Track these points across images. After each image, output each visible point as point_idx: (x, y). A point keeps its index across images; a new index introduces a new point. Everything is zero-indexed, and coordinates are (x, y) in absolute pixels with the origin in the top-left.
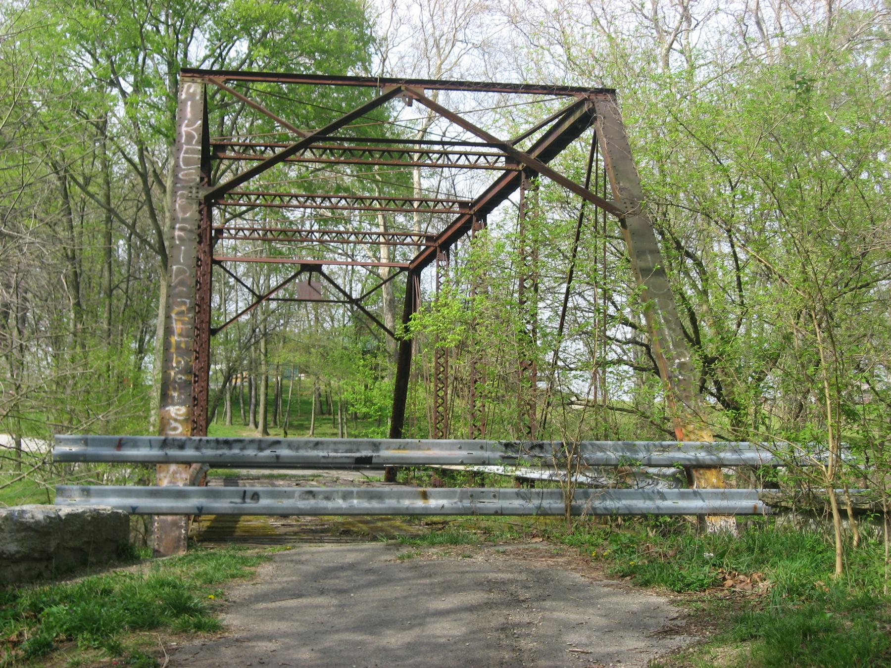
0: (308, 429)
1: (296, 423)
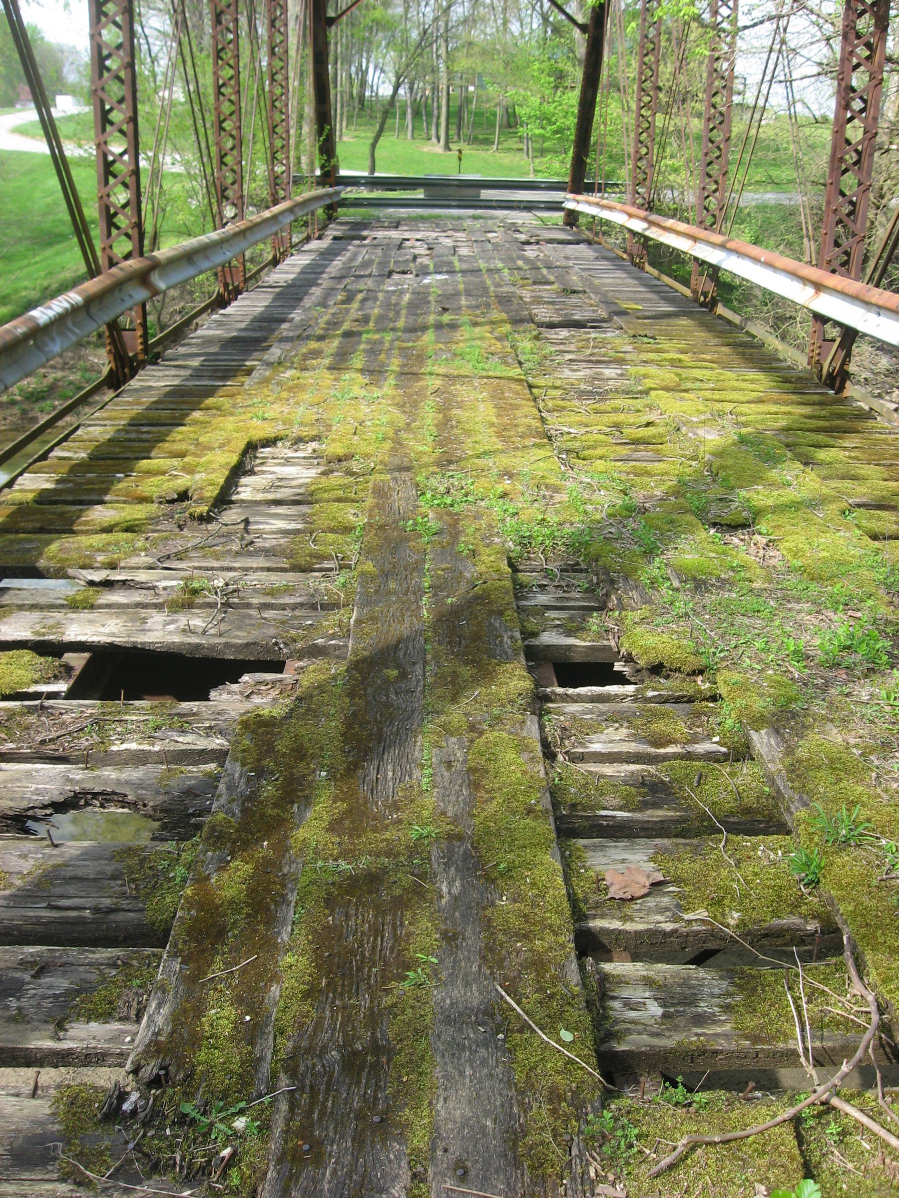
0: (493, 143)
1: (481, 137)
